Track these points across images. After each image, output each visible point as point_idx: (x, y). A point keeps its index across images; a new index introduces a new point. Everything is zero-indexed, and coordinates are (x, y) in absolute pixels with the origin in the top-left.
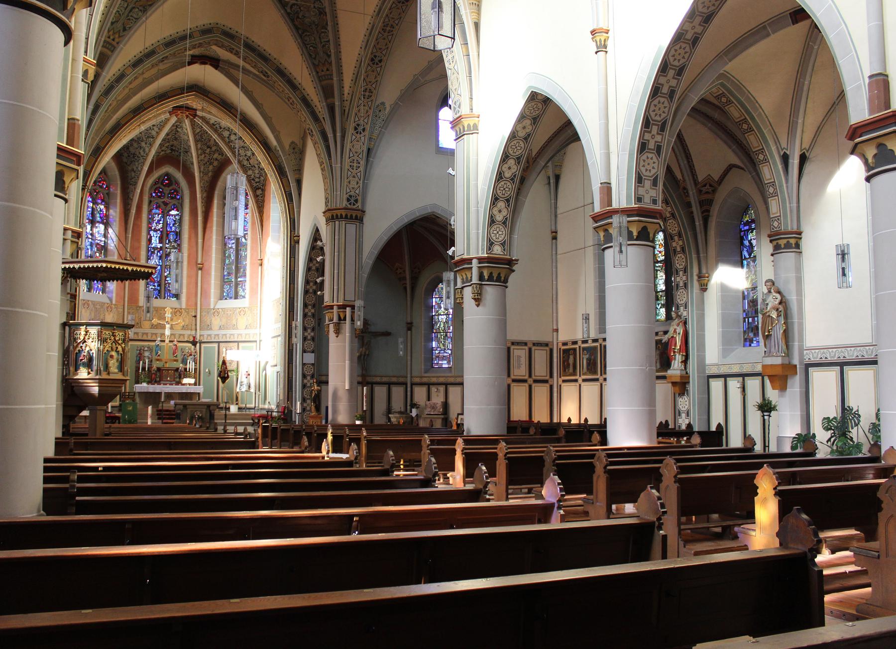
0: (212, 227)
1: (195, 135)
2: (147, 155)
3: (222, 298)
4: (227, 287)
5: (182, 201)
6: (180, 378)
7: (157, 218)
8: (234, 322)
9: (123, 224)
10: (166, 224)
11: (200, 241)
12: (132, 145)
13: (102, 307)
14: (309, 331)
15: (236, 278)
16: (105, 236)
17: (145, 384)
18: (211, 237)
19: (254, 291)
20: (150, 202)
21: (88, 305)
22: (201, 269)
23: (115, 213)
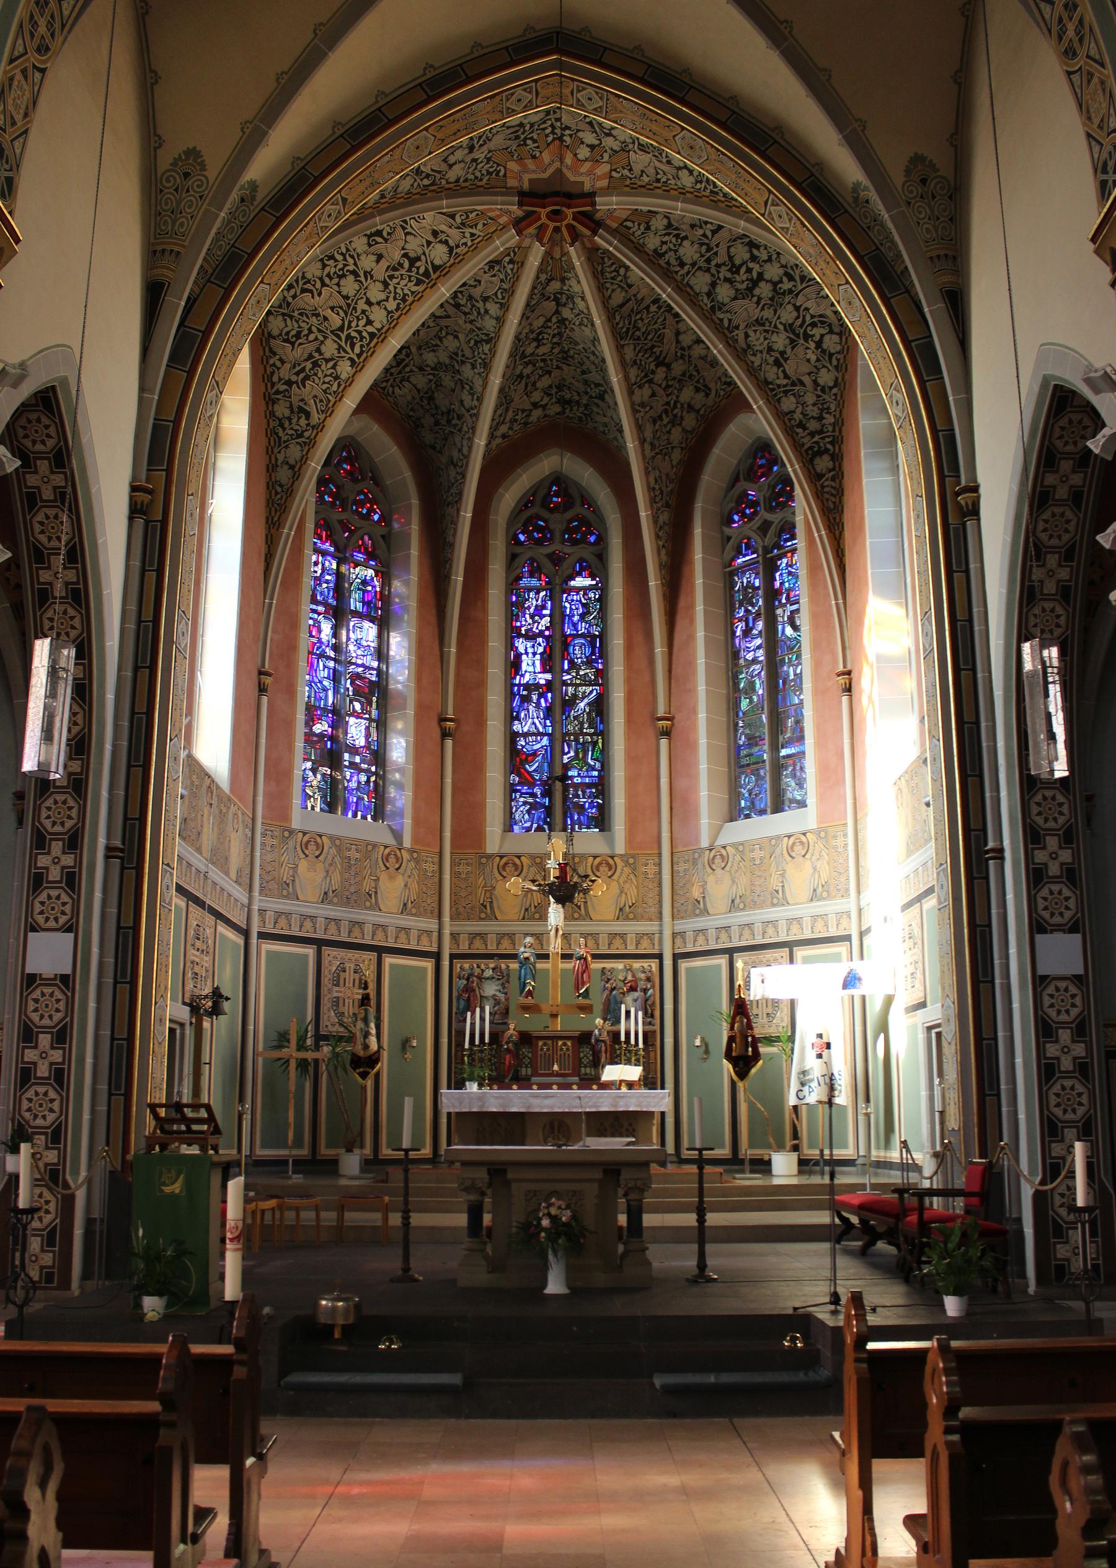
0: (691, 606)
1: (610, 313)
2: (480, 399)
3: (734, 814)
4: (748, 781)
5: (606, 548)
6: (597, 1065)
7: (533, 602)
8: (774, 883)
9: (433, 619)
10: (559, 617)
11: (659, 650)
12: (439, 385)
13: (367, 856)
14: (1052, 842)
15: (775, 747)
16: (381, 653)
17: (473, 1087)
18: (692, 637)
19: (830, 777)
20: (512, 558)
21: (320, 847)
22: (667, 733)
23: (406, 589)
